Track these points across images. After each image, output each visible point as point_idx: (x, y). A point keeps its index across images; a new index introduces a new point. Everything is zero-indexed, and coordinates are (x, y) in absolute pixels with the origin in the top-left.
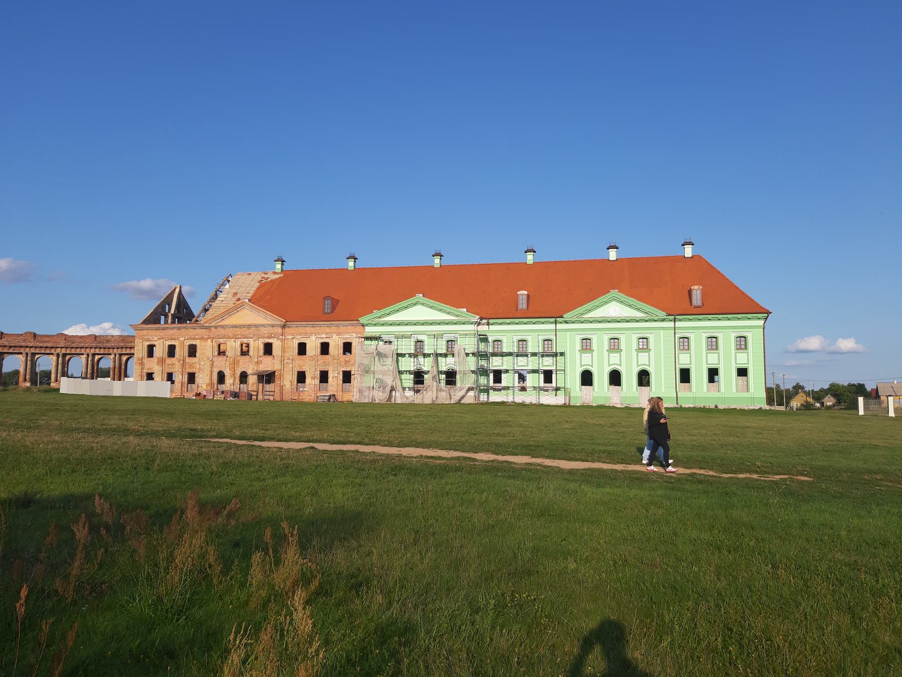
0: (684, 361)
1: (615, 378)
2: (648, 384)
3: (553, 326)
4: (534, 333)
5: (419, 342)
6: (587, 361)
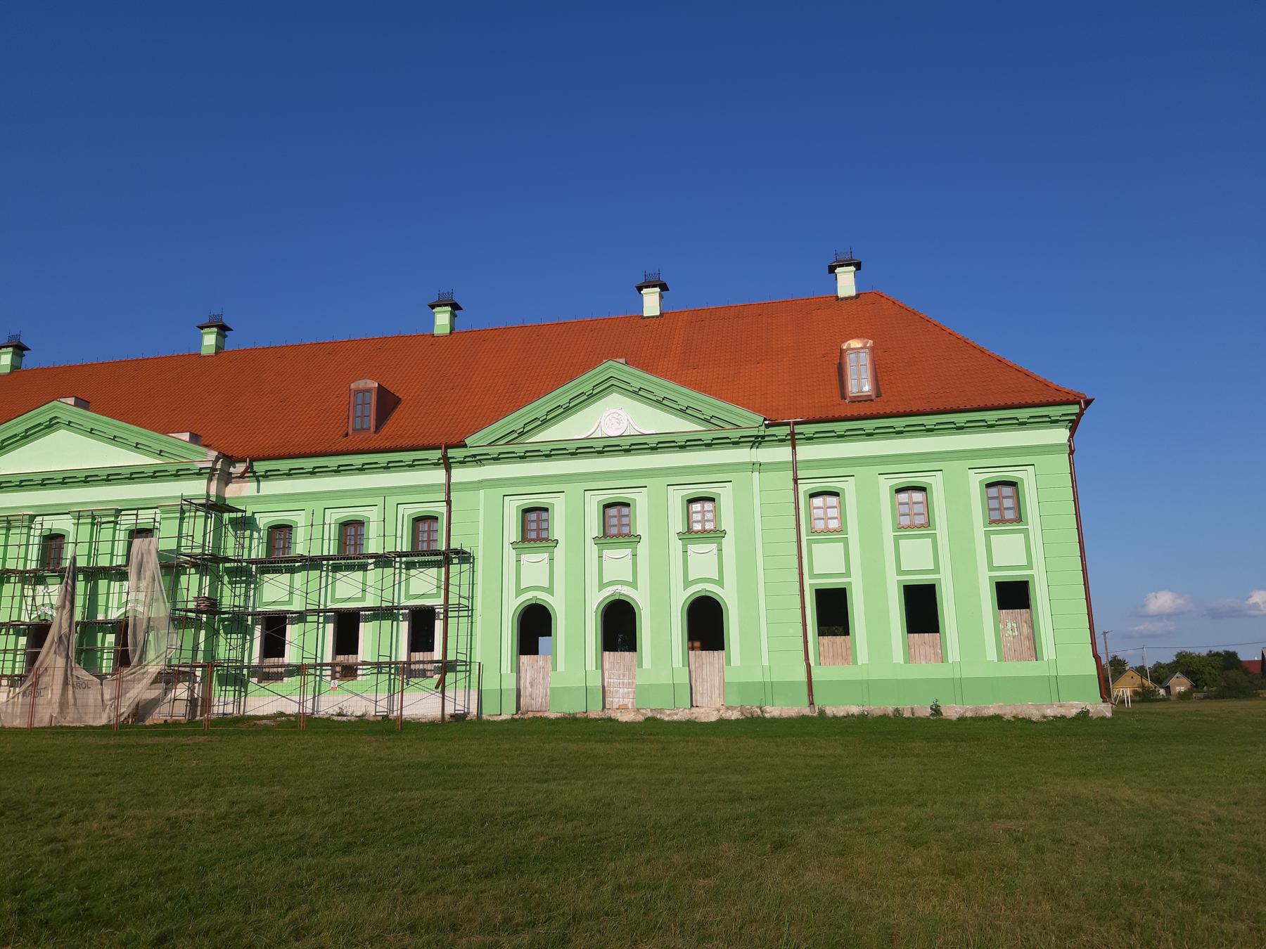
0: (827, 565)
1: (619, 626)
2: (630, 643)
3: (439, 476)
4: (386, 496)
5: (53, 541)
6: (534, 576)
